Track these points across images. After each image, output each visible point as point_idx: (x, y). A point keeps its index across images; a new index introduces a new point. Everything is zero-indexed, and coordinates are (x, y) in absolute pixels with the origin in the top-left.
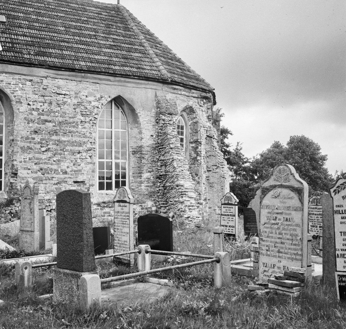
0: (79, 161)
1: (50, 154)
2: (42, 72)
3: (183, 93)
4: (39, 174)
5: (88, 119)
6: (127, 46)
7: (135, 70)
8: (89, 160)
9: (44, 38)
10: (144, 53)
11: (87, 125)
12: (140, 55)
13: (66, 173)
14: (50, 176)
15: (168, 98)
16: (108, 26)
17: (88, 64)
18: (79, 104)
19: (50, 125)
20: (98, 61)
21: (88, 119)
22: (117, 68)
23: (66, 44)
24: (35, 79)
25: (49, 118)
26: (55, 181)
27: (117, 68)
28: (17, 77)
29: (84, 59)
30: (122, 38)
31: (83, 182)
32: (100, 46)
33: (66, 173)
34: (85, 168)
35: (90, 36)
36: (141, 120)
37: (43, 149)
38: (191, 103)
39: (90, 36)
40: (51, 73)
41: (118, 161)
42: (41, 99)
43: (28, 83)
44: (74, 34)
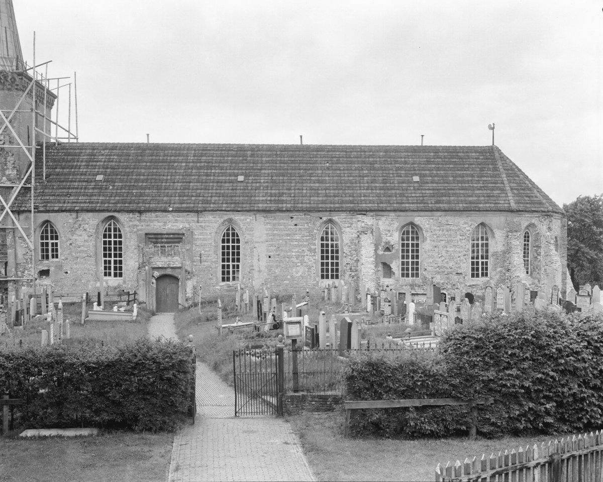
0: (459, 262)
1: (443, 258)
2: (439, 213)
3: (527, 215)
4: (438, 269)
5: (464, 238)
6: (492, 185)
7: (493, 205)
8: (465, 261)
9: (440, 189)
10: (503, 190)
11: (463, 241)
12: (499, 192)
13: (451, 268)
14: (443, 270)
15: (515, 220)
16: (482, 170)
17: (465, 205)
18: (459, 229)
19: (444, 242)
20: (471, 203)
21: (464, 238)
22: (481, 205)
23: (452, 191)
24: (434, 218)
25: (443, 239)
26: (446, 273)
27: (481, 205)
28: (426, 217)
29: (462, 202)
30: (490, 179)
31: (461, 274)
32: (473, 189)
33: (451, 268)
34: (463, 265)
35: (468, 182)
36: (496, 236)
37: (440, 256)
38: (533, 221)
39: (468, 182)
40: (443, 213)
41: (483, 260)
42: (438, 228)
43: (431, 220)
44: (459, 182)
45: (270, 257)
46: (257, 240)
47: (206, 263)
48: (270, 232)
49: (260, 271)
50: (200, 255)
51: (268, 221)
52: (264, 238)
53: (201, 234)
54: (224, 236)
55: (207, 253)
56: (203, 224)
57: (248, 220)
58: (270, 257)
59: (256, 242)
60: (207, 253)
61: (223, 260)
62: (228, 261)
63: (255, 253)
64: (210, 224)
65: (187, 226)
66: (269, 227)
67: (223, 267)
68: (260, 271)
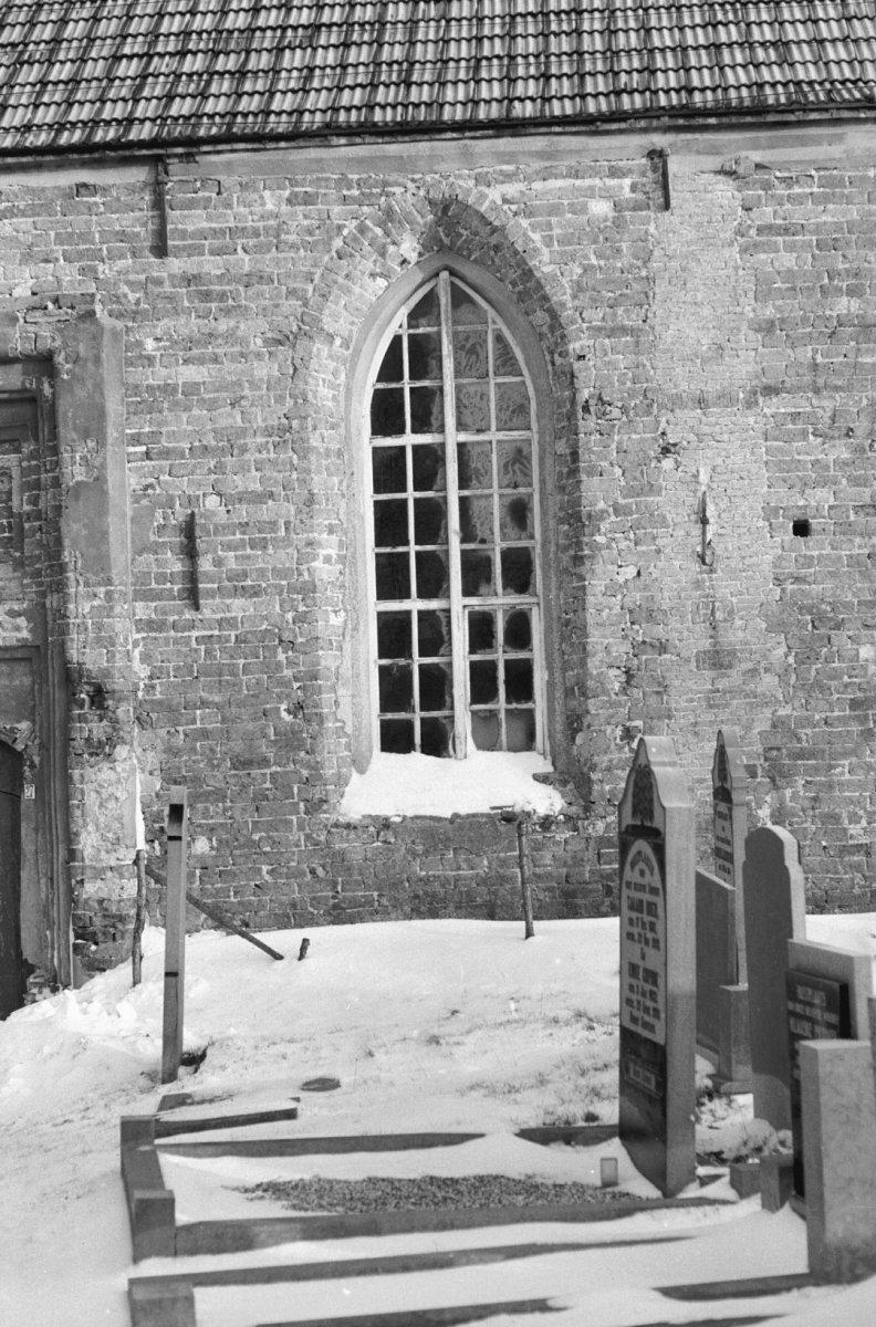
45: (802, 529)
46: (683, 381)
47: (239, 607)
48: (793, 307)
49: (717, 659)
50: (189, 529)
51: (765, 215)
52: (741, 369)
53: (189, 349)
54: (390, 369)
55: (243, 512)
56: (211, 265)
57: (600, 208)
58: (802, 529)
59: (677, 402)
60: (243, 512)
61: (391, 580)
62: (434, 583)
63: (672, 502)
64: (268, 262)
65: (69, 278)
66: (788, 260)
67: (393, 634)
68: (717, 659)
